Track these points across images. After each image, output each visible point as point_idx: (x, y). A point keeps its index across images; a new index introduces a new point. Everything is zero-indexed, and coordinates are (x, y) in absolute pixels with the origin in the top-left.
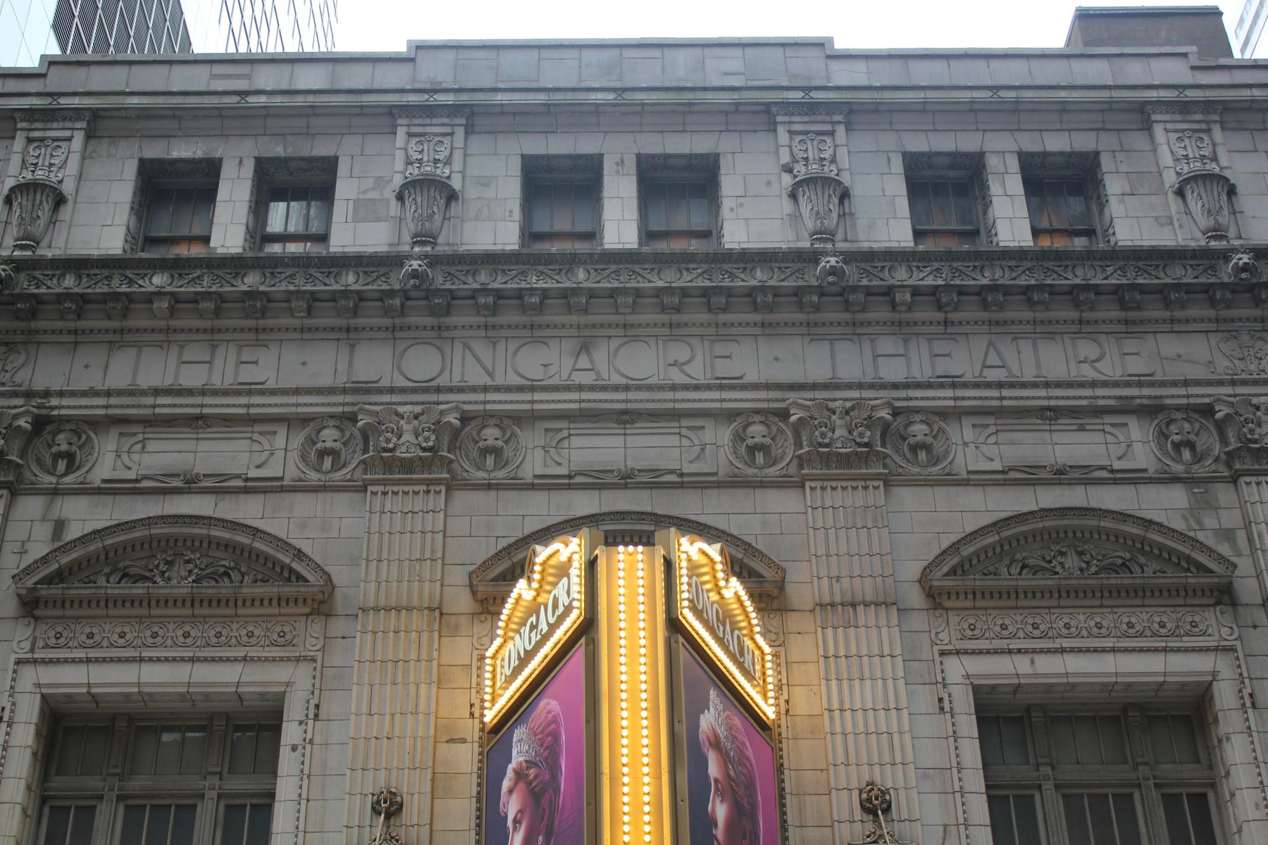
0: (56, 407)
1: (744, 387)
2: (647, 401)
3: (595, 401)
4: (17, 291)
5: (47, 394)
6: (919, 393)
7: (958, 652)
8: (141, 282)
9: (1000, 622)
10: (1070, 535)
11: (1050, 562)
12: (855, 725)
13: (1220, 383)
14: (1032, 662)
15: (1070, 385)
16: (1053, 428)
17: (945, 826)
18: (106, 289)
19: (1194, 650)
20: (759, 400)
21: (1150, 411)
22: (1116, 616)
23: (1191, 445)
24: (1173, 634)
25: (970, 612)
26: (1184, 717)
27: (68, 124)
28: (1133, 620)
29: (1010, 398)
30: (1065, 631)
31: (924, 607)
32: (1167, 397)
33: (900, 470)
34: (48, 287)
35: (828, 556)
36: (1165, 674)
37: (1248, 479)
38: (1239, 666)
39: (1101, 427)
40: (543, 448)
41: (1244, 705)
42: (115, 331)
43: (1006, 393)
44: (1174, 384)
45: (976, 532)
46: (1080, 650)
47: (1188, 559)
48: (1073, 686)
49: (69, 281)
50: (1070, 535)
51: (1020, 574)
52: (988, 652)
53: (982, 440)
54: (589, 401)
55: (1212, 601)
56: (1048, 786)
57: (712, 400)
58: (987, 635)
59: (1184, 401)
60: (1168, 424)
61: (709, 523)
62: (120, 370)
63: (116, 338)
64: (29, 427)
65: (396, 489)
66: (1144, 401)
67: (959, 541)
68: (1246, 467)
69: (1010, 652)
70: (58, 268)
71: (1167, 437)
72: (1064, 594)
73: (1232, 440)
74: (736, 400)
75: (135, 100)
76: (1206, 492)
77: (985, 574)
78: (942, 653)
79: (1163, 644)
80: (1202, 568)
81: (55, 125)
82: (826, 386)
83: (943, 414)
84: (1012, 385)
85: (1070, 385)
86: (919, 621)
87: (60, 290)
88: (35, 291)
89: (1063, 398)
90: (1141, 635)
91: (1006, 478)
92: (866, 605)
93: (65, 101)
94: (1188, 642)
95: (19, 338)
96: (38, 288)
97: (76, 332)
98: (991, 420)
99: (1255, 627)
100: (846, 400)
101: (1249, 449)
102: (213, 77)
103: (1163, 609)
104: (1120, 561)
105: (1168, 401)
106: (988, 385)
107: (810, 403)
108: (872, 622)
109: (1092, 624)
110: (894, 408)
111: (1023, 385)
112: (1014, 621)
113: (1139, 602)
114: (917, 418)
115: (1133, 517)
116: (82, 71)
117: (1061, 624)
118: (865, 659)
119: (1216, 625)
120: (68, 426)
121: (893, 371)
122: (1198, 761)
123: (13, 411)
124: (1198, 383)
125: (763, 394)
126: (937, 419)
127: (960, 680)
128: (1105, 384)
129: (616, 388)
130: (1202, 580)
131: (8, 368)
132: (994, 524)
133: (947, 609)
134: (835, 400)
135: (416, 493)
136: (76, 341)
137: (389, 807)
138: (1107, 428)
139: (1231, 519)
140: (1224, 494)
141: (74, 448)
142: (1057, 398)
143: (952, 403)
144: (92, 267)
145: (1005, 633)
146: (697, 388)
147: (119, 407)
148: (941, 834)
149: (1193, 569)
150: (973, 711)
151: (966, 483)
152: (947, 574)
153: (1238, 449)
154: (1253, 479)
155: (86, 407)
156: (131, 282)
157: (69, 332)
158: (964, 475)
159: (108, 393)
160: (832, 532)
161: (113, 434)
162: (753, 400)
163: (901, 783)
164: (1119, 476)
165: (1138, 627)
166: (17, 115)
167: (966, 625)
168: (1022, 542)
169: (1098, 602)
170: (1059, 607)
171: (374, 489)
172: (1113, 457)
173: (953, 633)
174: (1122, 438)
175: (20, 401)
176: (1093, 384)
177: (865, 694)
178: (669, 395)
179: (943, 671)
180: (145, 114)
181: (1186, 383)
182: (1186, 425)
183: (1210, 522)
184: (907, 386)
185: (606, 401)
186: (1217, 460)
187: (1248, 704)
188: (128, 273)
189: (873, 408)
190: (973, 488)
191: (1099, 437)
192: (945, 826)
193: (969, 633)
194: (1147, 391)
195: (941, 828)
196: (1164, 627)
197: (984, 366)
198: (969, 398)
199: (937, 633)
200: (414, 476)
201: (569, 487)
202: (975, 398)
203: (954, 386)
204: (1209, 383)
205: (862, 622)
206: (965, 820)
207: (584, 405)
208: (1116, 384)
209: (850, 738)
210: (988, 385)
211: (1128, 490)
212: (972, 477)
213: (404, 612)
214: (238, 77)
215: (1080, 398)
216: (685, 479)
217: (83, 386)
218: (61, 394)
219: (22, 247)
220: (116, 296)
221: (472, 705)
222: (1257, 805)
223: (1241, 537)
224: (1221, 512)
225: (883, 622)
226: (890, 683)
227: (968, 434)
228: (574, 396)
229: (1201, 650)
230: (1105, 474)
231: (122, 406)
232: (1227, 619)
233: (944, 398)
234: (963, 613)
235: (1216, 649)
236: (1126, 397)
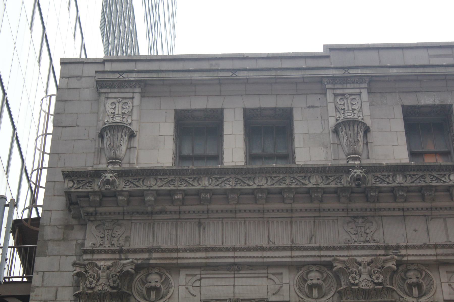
0: (405, 256)
4: (369, 185)
5: (398, 247)
8: (443, 179)
18: (423, 184)
27: (356, 85)
34: (388, 183)
42: (427, 209)
49: (399, 179)
62: (438, 233)
63: (428, 213)
64: (395, 267)
70: (390, 171)
75: (395, 71)
81: (348, 86)
87: (396, 184)
88: (380, 185)
93: (352, 72)
95: (369, 213)
96: (381, 183)
97: (403, 210)
102: (430, 56)
116: (350, 55)
120: (412, 267)
123: (383, 258)
131: (368, 231)
136: (404, 215)
141: (421, 281)
144: (411, 170)
147: (443, 255)
155: (424, 255)
156: (437, 179)
157: (399, 209)
159: (436, 247)
161: (442, 271)
166: (325, 80)
175: (382, 252)
180: (399, 79)
188: (434, 173)
214: (445, 56)
217: (420, 242)
218: (406, 247)
219: (112, 163)
220: (430, 188)
231: (446, 255)
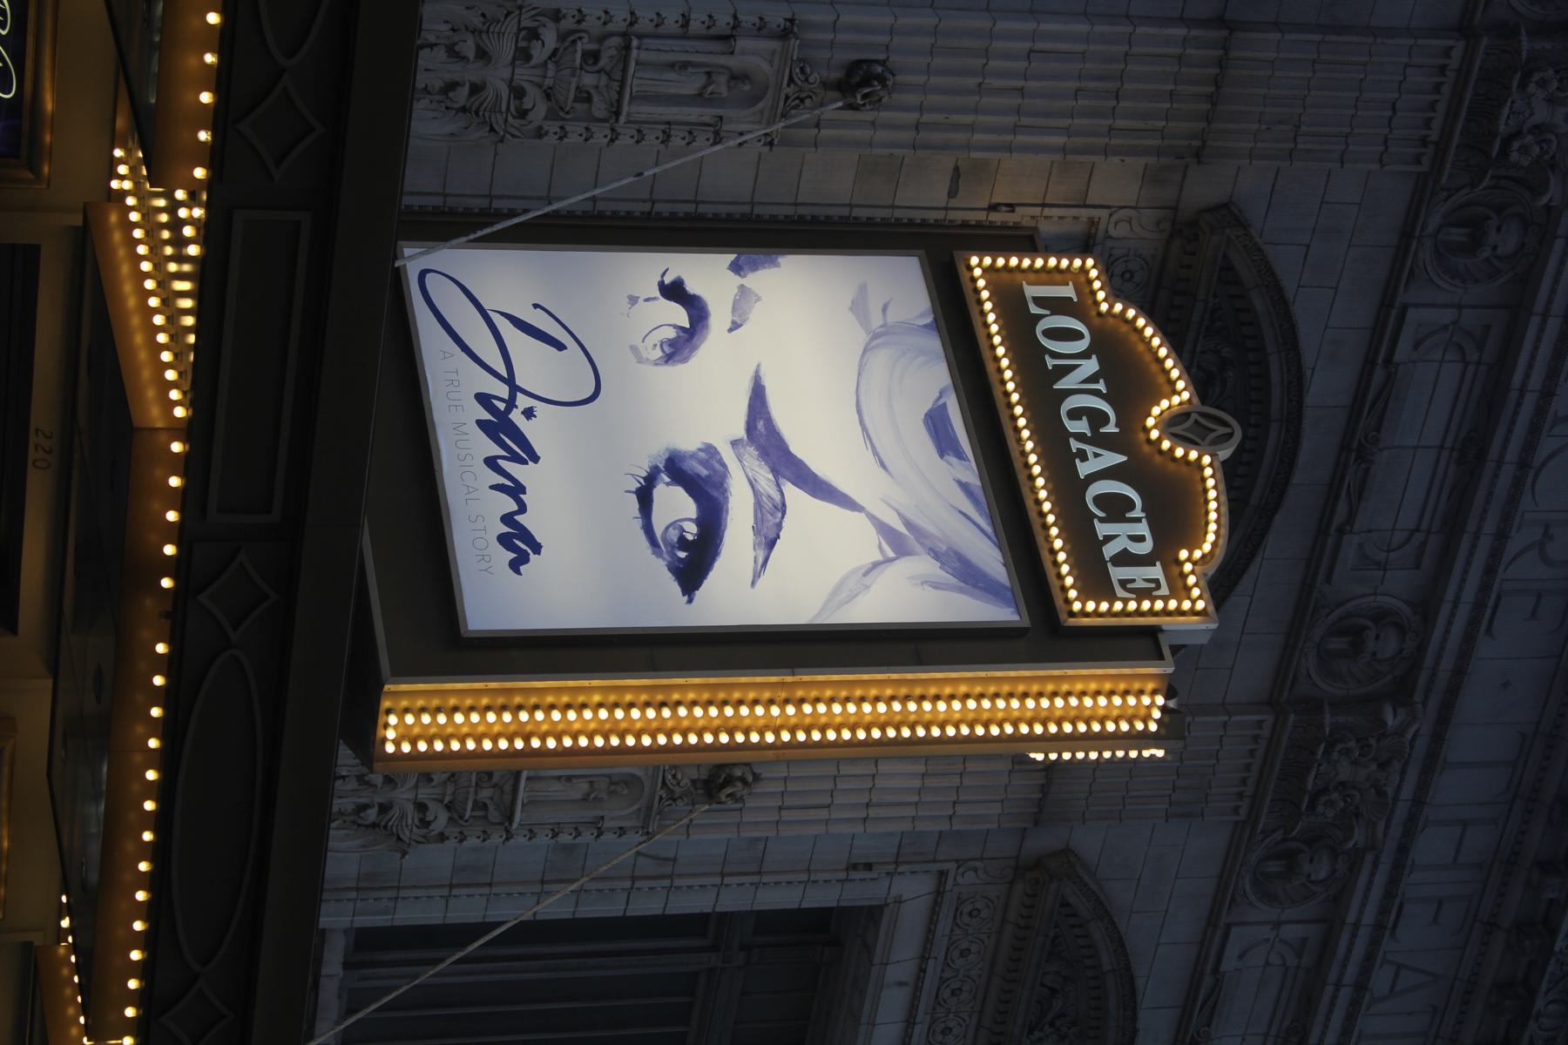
1: (1469, 639)
2: (1491, 493)
3: (1516, 413)
6: (1380, 879)
7: (939, 893)
9: (974, 948)
14: (901, 984)
17: (674, 860)
20: (1439, 657)
40: (1455, 323)
43: (1345, 993)
45: (1122, 945)
51: (1042, 985)
54: (1519, 404)
57: (1460, 589)
61: (1239, 588)
65: (1446, 89)
69: (924, 958)
74: (1450, 623)
78: (942, 875)
84: (1355, 1003)
92: (1044, 789)
107: (1409, 736)
111: (1351, 1018)
118: (956, 781)
121: (1431, 845)
125: (1447, 663)
127: (894, 892)
129: (1530, 446)
132: (1128, 968)
134: (1403, 773)
135: (1427, 123)
137: (860, 81)
143: (1351, 919)
146: (1490, 570)
150: (842, 904)
162: (1442, 648)
171: (1457, 54)
178: (1490, 527)
185: (1510, 431)
192: (674, 860)
193: (967, 908)
195: (672, 855)
197: (1400, 967)
199: (976, 870)
200: (1459, 126)
201: (1369, 362)
203: (1379, 927)
206: (678, 888)
207: (1514, 395)
213: (1207, 106)
216: (1330, 541)
221: (1011, 207)
226: (910, 811)
227: (1292, 932)
228: (1536, 381)
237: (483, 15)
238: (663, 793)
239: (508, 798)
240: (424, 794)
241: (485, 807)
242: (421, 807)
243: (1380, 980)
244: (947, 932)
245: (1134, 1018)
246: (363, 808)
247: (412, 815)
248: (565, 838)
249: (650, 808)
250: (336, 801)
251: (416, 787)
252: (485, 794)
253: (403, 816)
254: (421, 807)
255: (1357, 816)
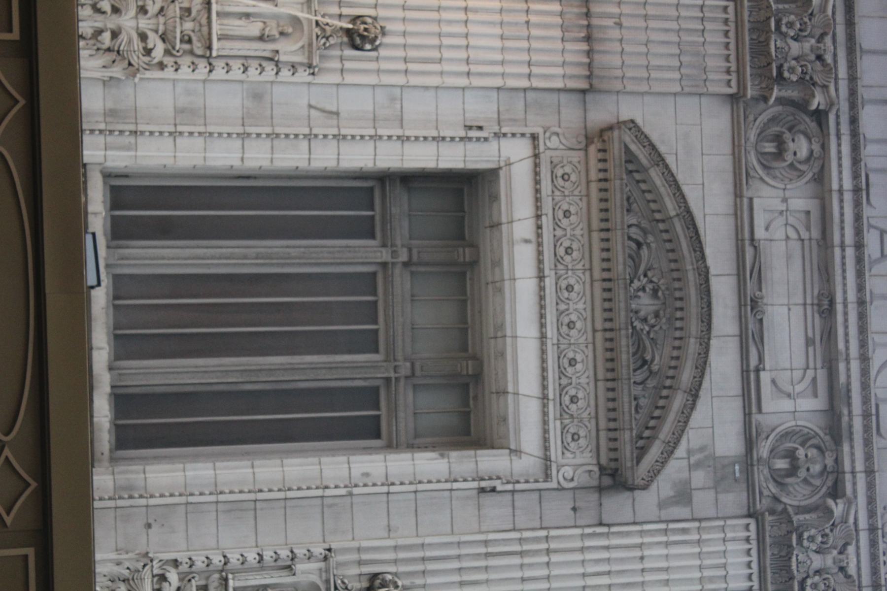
6: (846, 149)
7: (536, 156)
10: (678, 304)
11: (645, 275)
12: (450, 22)
13: (872, 514)
14: (527, 241)
15: (863, 329)
16: (809, 308)
17: (337, 114)
19: (546, 431)
21: (835, 429)
22: (583, 347)
23: (793, 471)
24: (563, 411)
25: (583, 174)
26: (468, 417)
28: (579, 366)
29: (843, 257)
30: (563, 284)
31: (589, 125)
32: (852, 447)
33: (751, 118)
35: (646, 17)
36: (516, 394)
37: (753, 527)
38: (527, 482)
39: (811, 365)
41: (482, 479)
43: (850, 252)
44: (869, 457)
46: (542, 298)
47: (651, 439)
48: (500, 290)
50: (678, 304)
51: (630, 238)
52: (537, 191)
53: (791, 220)
55: (604, 461)
56: (385, 255)
58: (557, 193)
59: (847, 467)
60: (818, 448)
66: (845, 419)
67: (667, 167)
68: (768, 528)
69: (538, 217)
71: (803, 444)
72: (607, 285)
73: (801, 517)
76: (736, 480)
77: (628, 199)
78: (534, 137)
79: (551, 396)
80: (642, 451)
82: (851, 38)
83: (821, 178)
84: (859, 260)
85: (863, 329)
86: (571, 115)
89: (846, 320)
90: (562, 373)
91: (745, 242)
92: (589, 53)
94: (555, 427)
98: (816, 233)
99: (574, 509)
100: (835, 55)
101: (790, 532)
103: (592, 403)
104: (648, 357)
105: (846, 448)
106: (859, 232)
107: (829, 12)
108: (569, 58)
109: (574, 317)
110: (826, 113)
111: (860, 274)
112: (575, 226)
113: (601, 375)
114: (816, 147)
115: (702, 376)
117: (572, 281)
118: (525, 44)
119: (576, 464)
122: (416, 436)
124: (871, 486)
126: (816, 170)
127: (505, 153)
128: (865, 372)
130: (628, 448)
132: (688, 211)
133: (586, 150)
138: (810, 373)
139: (703, 502)
140: (734, 500)
142: (846, 314)
143: (835, 186)
145: (560, 214)
148: (329, 107)
149: (641, 443)
151: (738, 194)
152: (626, 147)
153: (790, 521)
154: (753, 534)
158: (747, 194)
160: (674, 25)
163: (384, 65)
164: (752, 376)
165: (570, 370)
167: (568, 169)
168: (668, 246)
169: (599, 325)
170: (592, 281)
172: (774, 374)
173: (558, 153)
174: (799, 388)
176: (864, 359)
177: (486, 40)
179: (514, 135)
181: (870, 472)
182: (816, 468)
183: (699, 478)
184: (855, 134)
186: (776, 499)
187: (483, 484)
189: (825, 87)
190: (732, 203)
191: (799, 361)
192: (337, 114)
193: (560, 172)
194: (858, 424)
195: (334, 109)
196: (572, 401)
198: (842, 208)
199: (557, 134)
202: (842, 215)
203: (857, 190)
204: (871, 500)
205: (569, 46)
208: (865, 386)
209: (434, 15)
210: (859, 232)
211: (734, 385)
212: (745, 201)
215: (847, 341)
222: (367, 475)
223: (684, 512)
224: (712, 493)
225: (570, 71)
226: (498, 69)
229: (546, 440)
230: (753, 362)
232: (582, 478)
233: (841, 177)
234: (581, 167)
235: (547, 458)
236: (849, 398)
237: (128, 568)
238: (317, 30)
239: (205, 29)
240: (144, 23)
241: (190, 41)
242: (143, 37)
243: (872, 240)
244: (550, 193)
245: (703, 257)
246: (99, 32)
247: (137, 44)
248: (253, 72)
249: (310, 45)
250: (81, 24)
251: (136, 17)
252: (188, 25)
253: (130, 41)
254: (143, 37)
255: (813, 84)
